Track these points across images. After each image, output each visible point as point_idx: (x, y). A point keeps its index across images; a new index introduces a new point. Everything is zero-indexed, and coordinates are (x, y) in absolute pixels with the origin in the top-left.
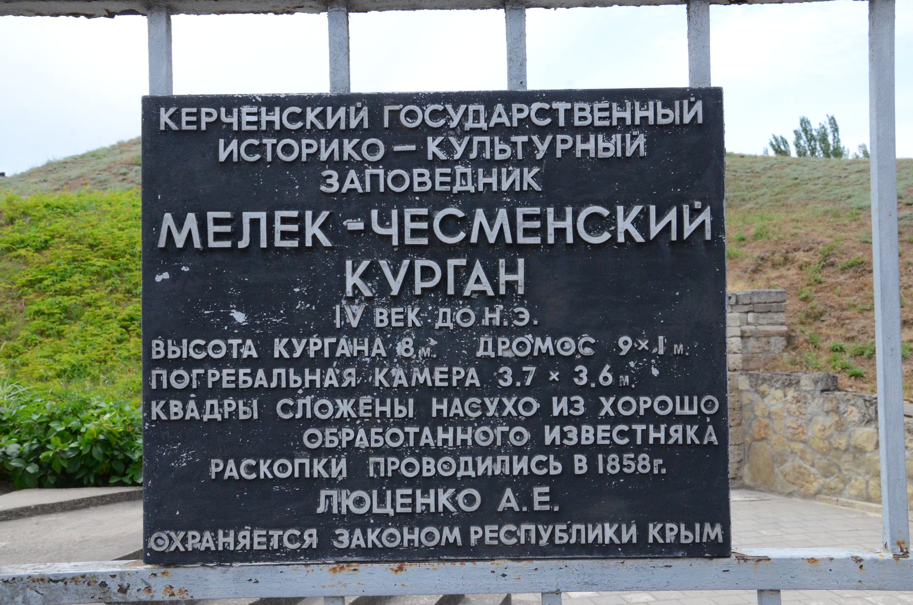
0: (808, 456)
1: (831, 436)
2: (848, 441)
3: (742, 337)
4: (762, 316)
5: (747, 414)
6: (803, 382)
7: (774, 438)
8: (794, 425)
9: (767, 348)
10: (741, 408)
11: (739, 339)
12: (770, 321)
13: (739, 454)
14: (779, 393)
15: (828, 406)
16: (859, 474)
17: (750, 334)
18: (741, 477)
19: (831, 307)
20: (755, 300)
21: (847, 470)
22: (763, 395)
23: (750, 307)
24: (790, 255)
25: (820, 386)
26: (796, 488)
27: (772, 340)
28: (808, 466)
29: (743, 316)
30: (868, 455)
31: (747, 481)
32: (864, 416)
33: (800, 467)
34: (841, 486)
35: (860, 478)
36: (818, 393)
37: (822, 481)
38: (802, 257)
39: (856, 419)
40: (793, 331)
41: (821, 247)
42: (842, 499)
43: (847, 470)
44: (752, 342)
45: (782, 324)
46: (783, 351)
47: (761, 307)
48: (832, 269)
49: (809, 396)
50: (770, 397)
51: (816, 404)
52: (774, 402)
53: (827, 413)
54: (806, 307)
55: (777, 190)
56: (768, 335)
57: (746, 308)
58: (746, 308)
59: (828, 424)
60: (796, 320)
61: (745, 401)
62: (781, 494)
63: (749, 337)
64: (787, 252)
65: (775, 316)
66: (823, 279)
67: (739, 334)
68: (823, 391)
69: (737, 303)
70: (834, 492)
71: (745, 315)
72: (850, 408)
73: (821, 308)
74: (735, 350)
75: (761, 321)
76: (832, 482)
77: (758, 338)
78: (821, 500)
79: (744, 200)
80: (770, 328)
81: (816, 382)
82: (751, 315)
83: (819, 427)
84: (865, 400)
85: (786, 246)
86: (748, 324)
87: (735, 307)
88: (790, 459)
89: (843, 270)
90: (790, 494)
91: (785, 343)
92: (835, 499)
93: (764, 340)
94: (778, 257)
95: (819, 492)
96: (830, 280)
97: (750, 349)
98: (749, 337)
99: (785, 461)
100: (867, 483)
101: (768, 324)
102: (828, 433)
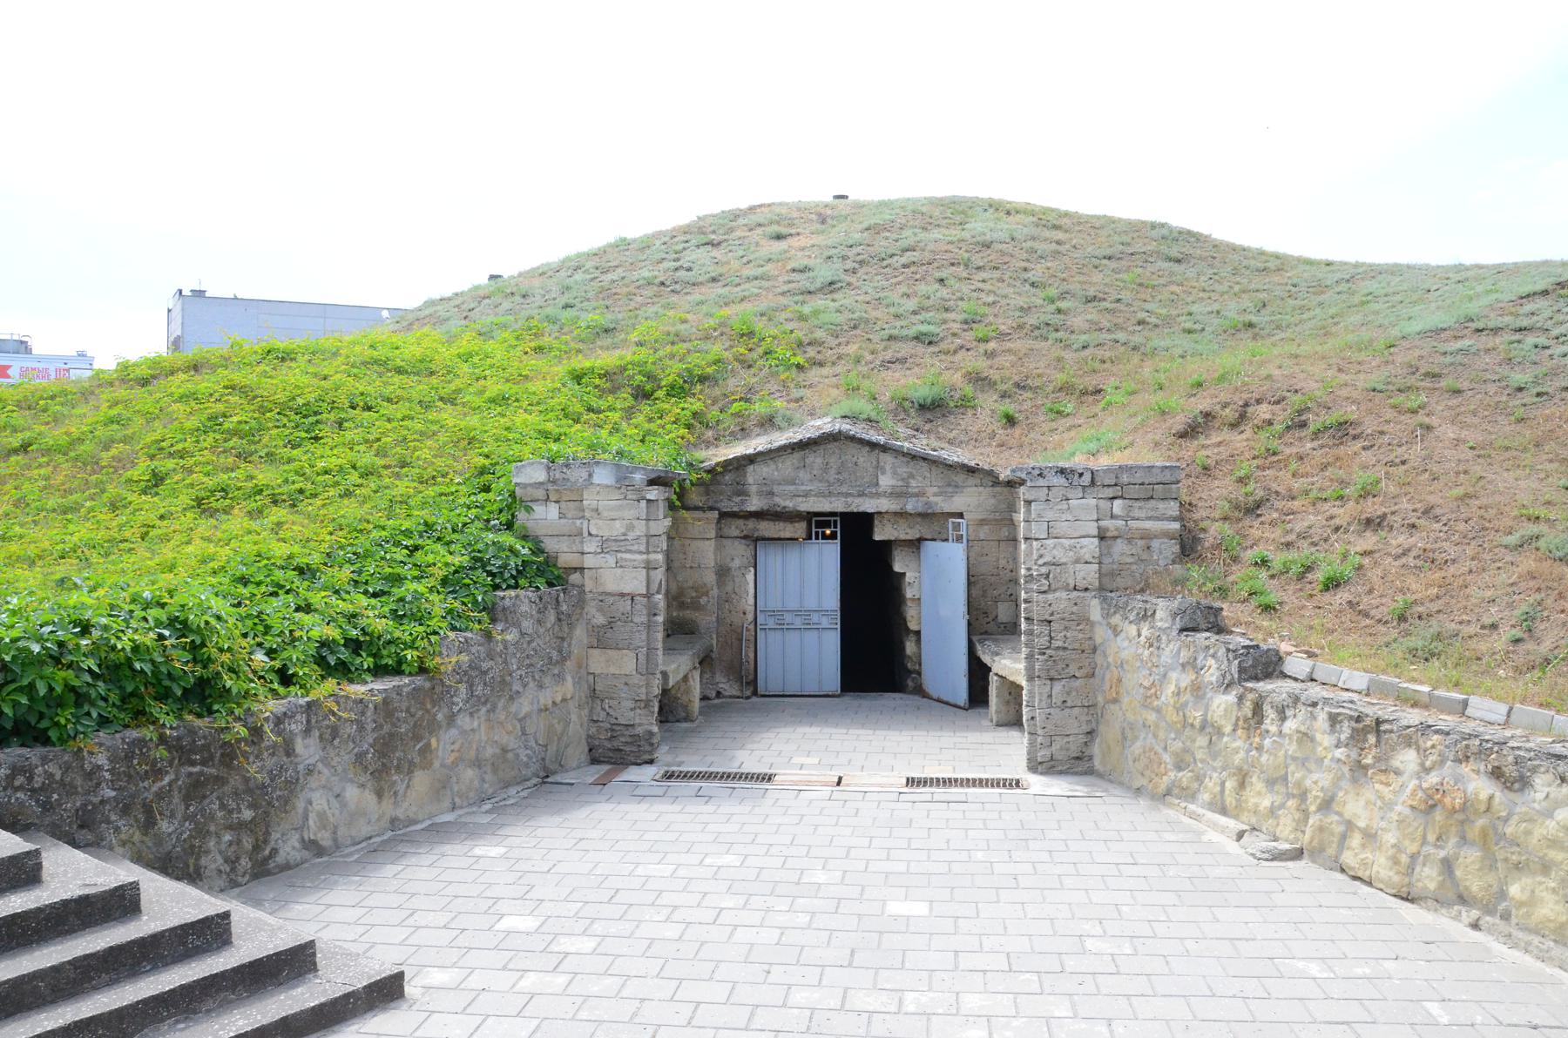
0: (1162, 735)
1: (1185, 705)
2: (1205, 715)
3: (1102, 538)
4: (1137, 504)
5: (1099, 659)
6: (1159, 614)
7: (1125, 700)
8: (1146, 683)
9: (1144, 557)
10: (1095, 650)
11: (1096, 541)
12: (1151, 514)
13: (1089, 722)
14: (1133, 630)
15: (1184, 655)
16: (1214, 769)
17: (1115, 533)
18: (1091, 758)
19: (1277, 493)
20: (1125, 478)
21: (1202, 761)
22: (1116, 631)
23: (1117, 491)
24: (1250, 410)
25: (1178, 624)
26: (1144, 782)
27: (1155, 544)
28: (1160, 751)
29: (1105, 505)
30: (1225, 739)
31: (1097, 763)
32: (1224, 676)
33: (1151, 749)
34: (1196, 785)
35: (1215, 775)
36: (1175, 633)
37: (1172, 774)
38: (1264, 411)
39: (1214, 679)
40: (1204, 530)
41: (1297, 398)
42: (1192, 807)
43: (1202, 761)
44: (1120, 547)
45: (1175, 519)
46: (1174, 562)
47: (1133, 491)
48: (1297, 433)
49: (1164, 638)
50: (1123, 635)
51: (1173, 649)
52: (1126, 644)
53: (1183, 666)
54: (1239, 494)
55: (1333, 311)
56: (1147, 536)
57: (1110, 492)
58: (1110, 492)
59: (1183, 685)
60: (1217, 514)
61: (1098, 640)
62: (1129, 788)
63: (1115, 538)
64: (1246, 405)
65: (1161, 505)
66: (1280, 448)
67: (1095, 532)
68: (1182, 630)
69: (1093, 483)
70: (1190, 795)
71: (1109, 503)
72: (1211, 661)
73: (1260, 494)
74: (1088, 557)
75: (1136, 513)
76: (1185, 777)
77: (1130, 540)
78: (1170, 805)
79: (1278, 327)
80: (1148, 525)
81: (1174, 615)
82: (1117, 503)
83: (1172, 688)
84: (1228, 650)
85: (1245, 396)
86: (1112, 517)
87: (1089, 490)
88: (1143, 735)
89: (1316, 435)
90: (1138, 791)
91: (1177, 549)
92: (1183, 805)
93: (1140, 543)
94: (1229, 414)
95: (1168, 793)
96: (1288, 451)
97: (1116, 557)
98: (1115, 538)
99: (1136, 738)
100: (1223, 784)
101: (1149, 518)
102: (1183, 699)
